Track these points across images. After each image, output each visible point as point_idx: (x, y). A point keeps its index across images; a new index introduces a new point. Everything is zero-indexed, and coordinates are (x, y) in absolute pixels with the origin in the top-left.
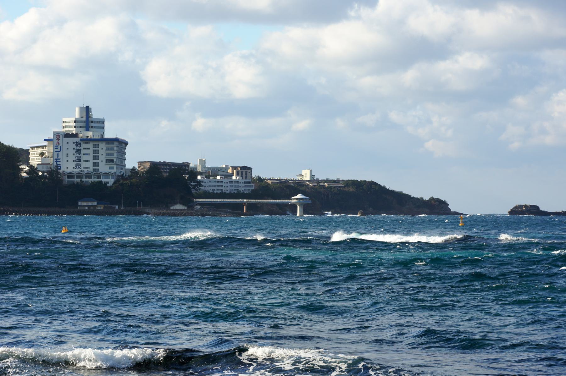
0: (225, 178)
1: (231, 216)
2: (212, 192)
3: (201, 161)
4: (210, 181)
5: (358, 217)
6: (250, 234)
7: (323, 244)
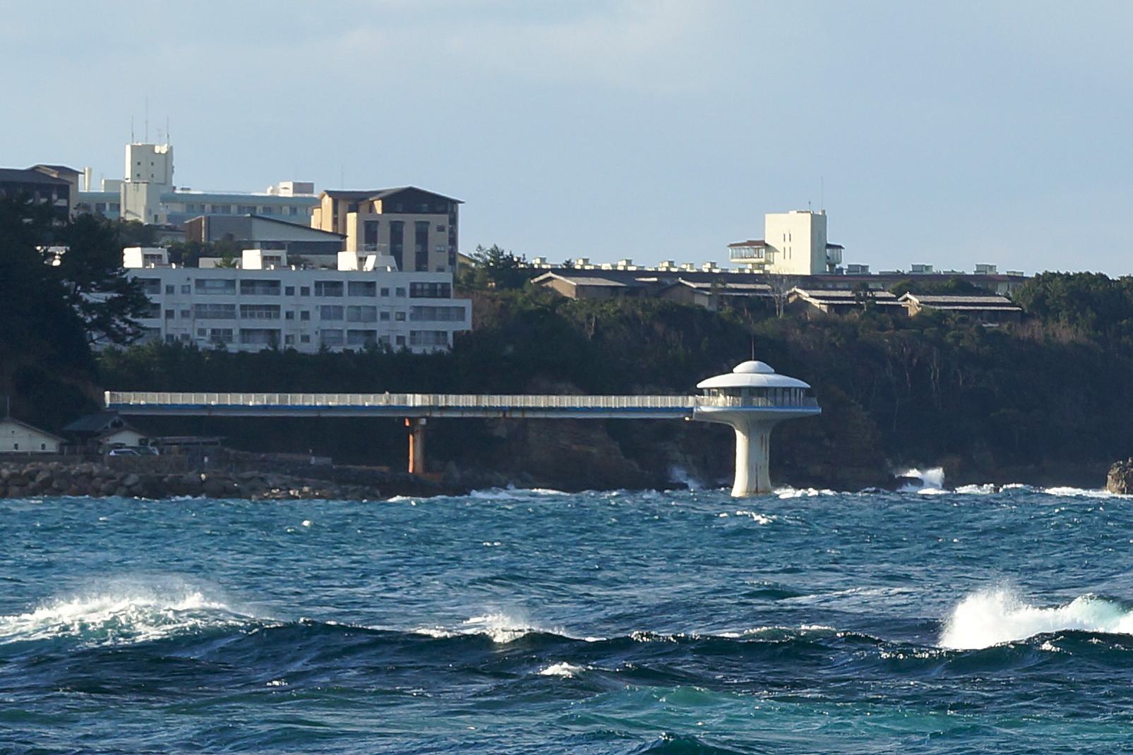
0: (290, 263)
1: (328, 499)
2: (213, 347)
3: (143, 156)
4: (200, 283)
5: (1106, 504)
6: (447, 608)
7: (893, 666)
